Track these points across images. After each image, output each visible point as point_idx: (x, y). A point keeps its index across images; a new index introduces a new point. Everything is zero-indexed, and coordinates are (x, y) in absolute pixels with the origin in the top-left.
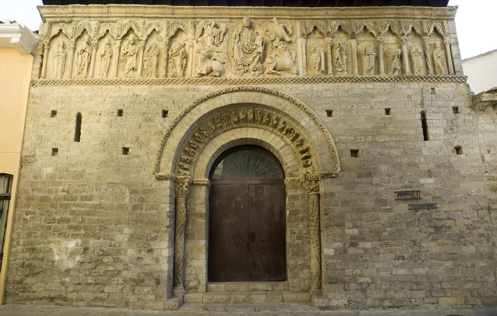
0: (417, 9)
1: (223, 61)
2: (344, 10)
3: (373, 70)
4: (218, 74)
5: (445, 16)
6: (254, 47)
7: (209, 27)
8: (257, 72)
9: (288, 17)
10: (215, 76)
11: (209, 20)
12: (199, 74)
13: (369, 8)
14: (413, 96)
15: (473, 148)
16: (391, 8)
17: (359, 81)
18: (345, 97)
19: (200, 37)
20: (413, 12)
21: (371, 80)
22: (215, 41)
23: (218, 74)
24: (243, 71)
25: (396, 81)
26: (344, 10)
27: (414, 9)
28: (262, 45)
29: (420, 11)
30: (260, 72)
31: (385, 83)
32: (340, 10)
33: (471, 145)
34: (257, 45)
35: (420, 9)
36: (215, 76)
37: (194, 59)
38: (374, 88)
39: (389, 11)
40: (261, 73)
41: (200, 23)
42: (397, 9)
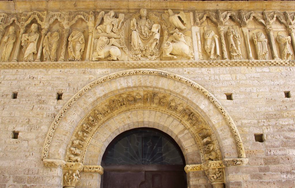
1: (120, 47)
4: (116, 59)
6: (151, 34)
7: (108, 17)
8: (154, 57)
10: (113, 60)
11: (108, 11)
12: (97, 58)
19: (99, 25)
22: (114, 28)
23: (116, 59)
24: (140, 55)
28: (158, 32)
30: (157, 57)
34: (153, 33)
36: (113, 60)
37: (93, 44)
40: (158, 57)
41: (100, 13)
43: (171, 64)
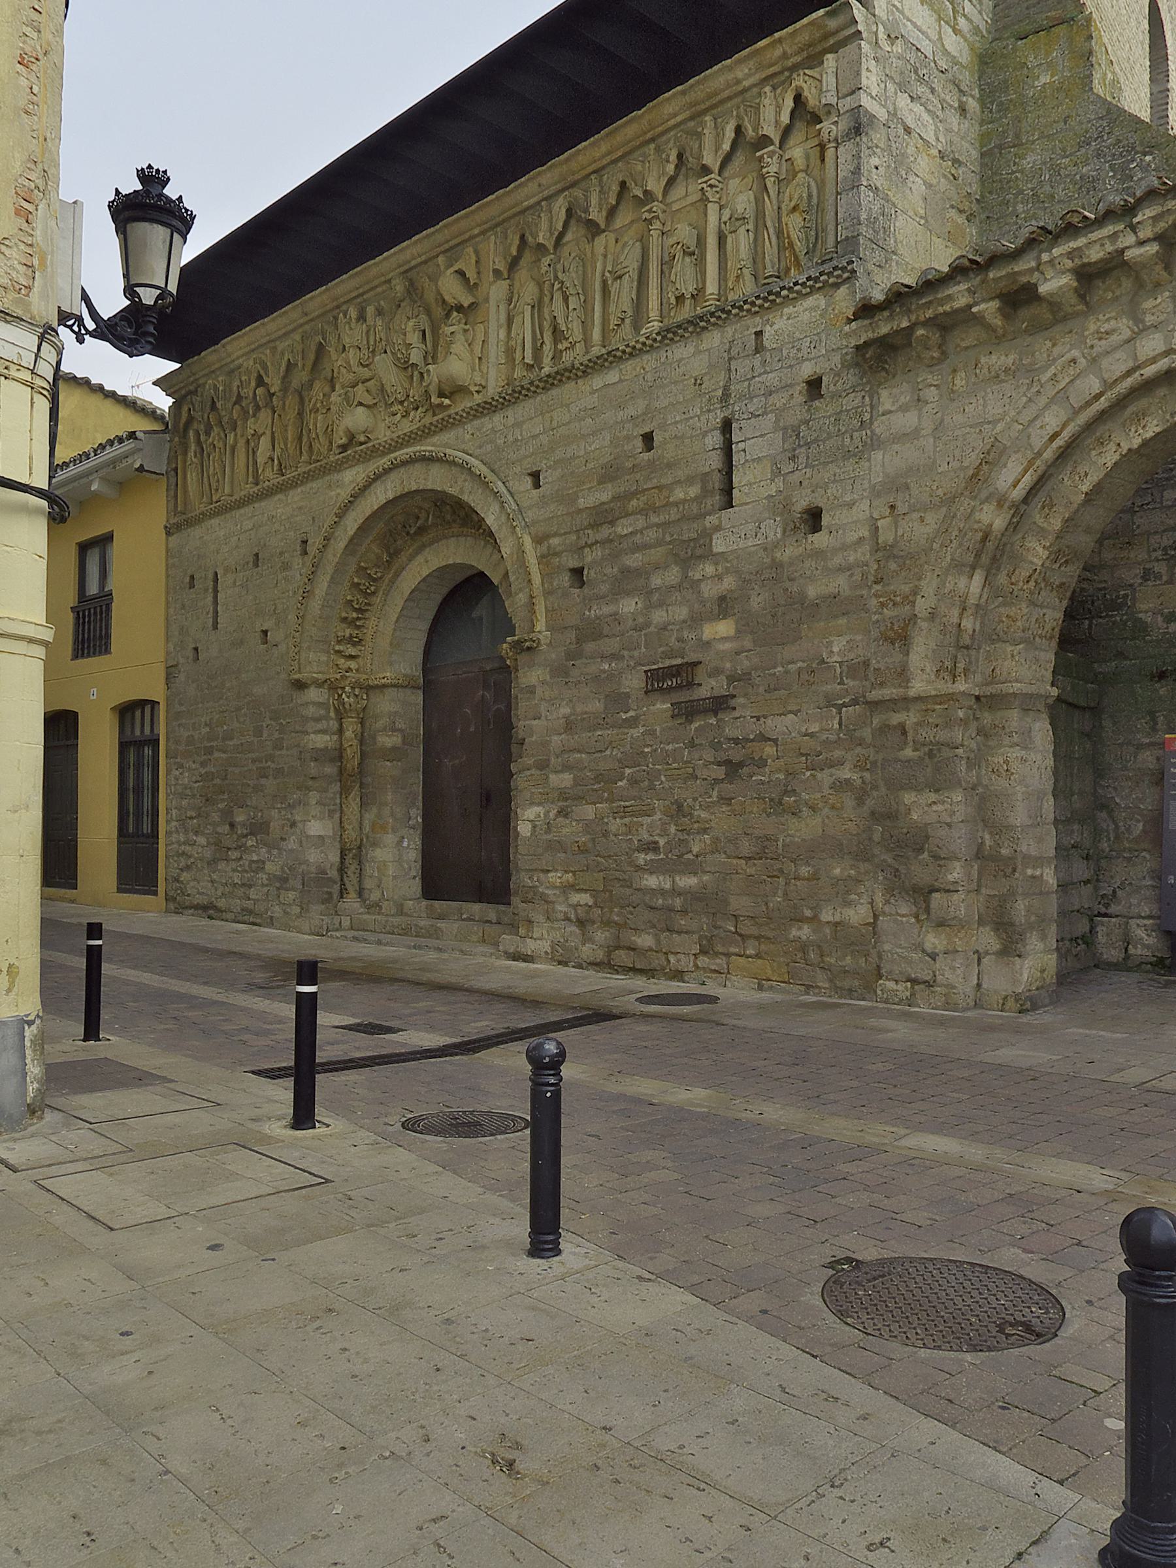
0: (740, 61)
2: (567, 160)
3: (627, 321)
5: (826, 37)
9: (476, 231)
13: (616, 129)
14: (705, 378)
15: (850, 505)
16: (668, 99)
17: (589, 371)
18: (564, 425)
20: (730, 76)
21: (611, 359)
25: (667, 341)
26: (567, 160)
27: (730, 68)
29: (752, 63)
31: (646, 357)
32: (561, 163)
33: (848, 498)
35: (748, 57)
38: (621, 381)
39: (669, 109)
42: (683, 93)
43: (448, 421)
